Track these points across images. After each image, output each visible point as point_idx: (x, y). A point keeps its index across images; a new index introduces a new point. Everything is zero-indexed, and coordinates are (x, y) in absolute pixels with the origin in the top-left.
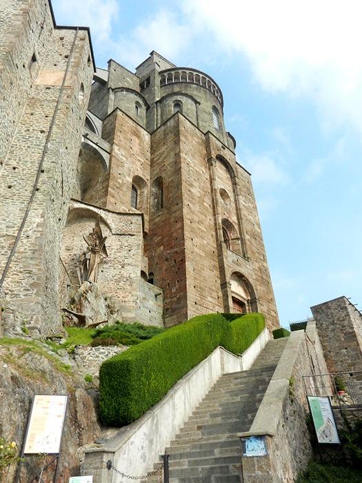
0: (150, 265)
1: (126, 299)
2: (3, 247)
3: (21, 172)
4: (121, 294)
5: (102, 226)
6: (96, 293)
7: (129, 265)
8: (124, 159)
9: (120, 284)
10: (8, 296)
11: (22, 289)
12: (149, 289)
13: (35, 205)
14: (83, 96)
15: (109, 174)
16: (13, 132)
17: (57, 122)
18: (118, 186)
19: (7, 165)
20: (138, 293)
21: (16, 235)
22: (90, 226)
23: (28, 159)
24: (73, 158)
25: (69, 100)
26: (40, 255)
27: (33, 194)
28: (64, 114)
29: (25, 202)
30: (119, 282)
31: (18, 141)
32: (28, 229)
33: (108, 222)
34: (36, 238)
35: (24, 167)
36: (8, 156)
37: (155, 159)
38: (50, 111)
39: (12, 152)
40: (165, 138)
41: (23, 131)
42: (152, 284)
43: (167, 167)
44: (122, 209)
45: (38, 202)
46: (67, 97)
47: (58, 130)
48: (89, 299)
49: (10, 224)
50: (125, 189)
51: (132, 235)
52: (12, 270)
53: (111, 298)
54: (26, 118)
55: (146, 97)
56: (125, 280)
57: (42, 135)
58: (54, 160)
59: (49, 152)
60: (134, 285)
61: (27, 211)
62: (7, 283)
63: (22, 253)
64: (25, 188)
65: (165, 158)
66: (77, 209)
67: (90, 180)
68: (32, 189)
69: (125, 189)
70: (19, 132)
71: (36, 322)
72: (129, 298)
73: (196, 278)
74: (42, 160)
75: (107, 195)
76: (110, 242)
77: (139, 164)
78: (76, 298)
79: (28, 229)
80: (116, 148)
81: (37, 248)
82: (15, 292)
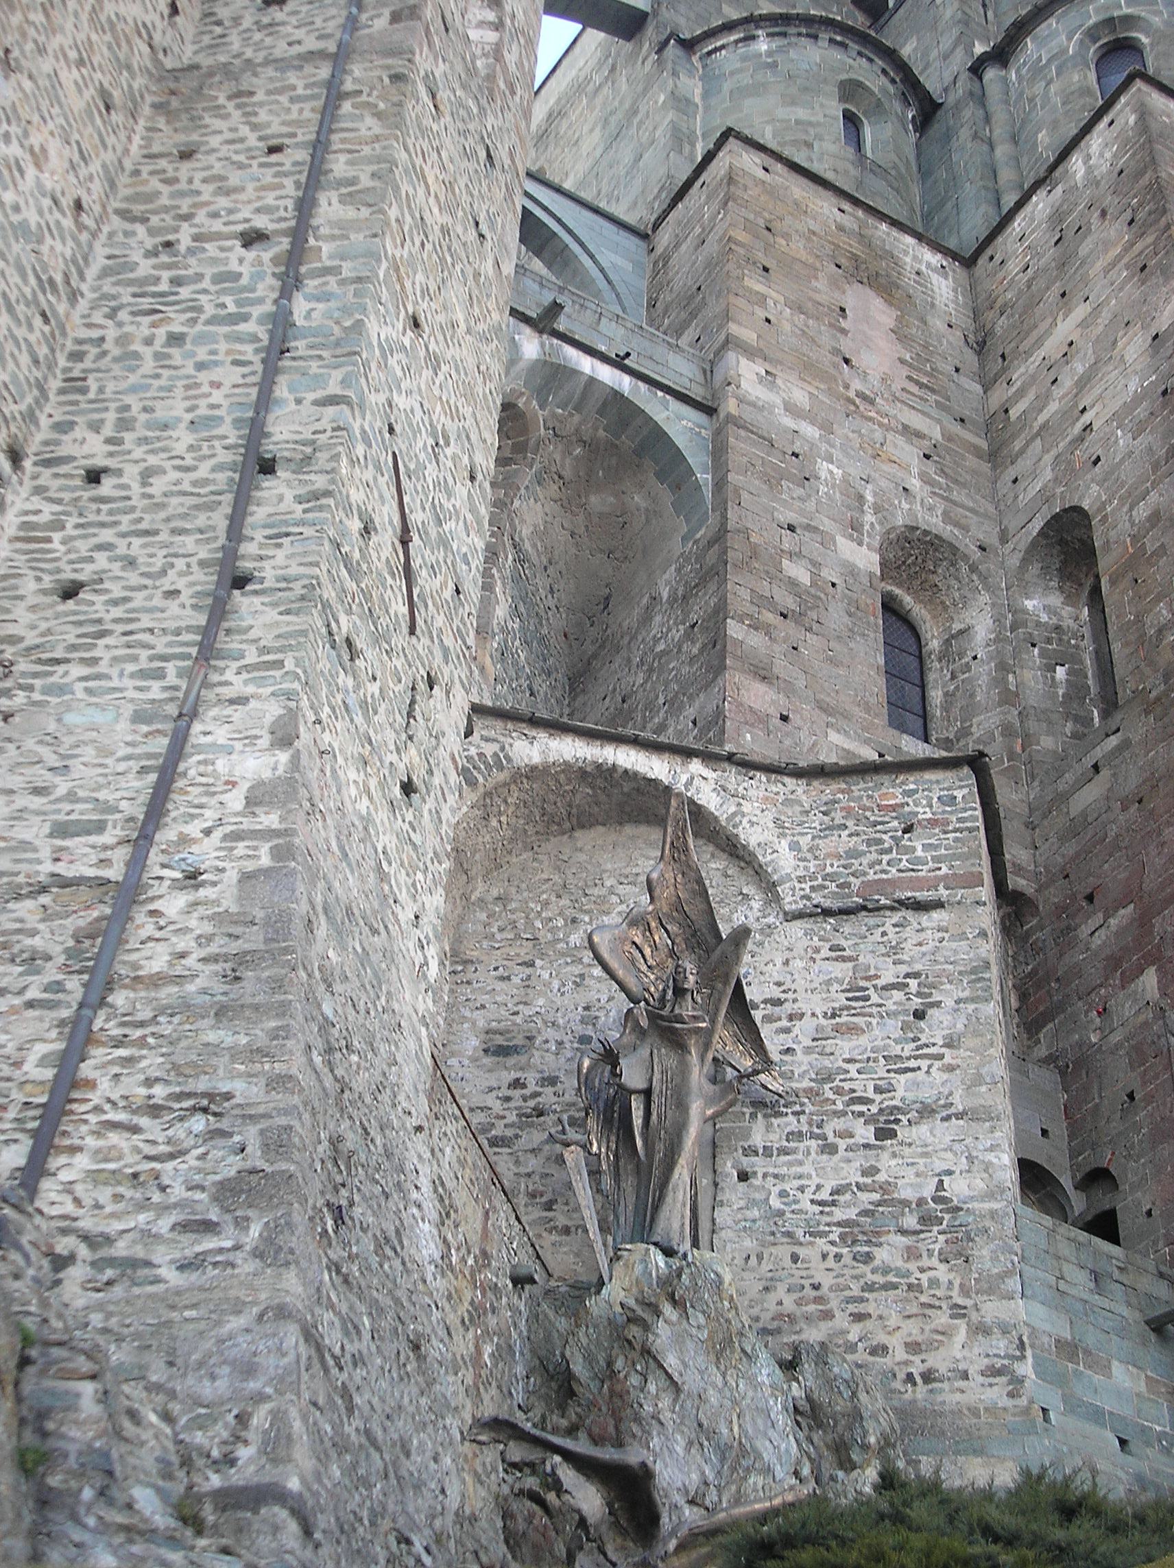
0: (1077, 1119)
1: (938, 1361)
2: (33, 961)
3: (136, 490)
4: (894, 1325)
5: (713, 867)
6: (715, 1317)
7: (926, 1111)
8: (810, 431)
10: (76, 1274)
11: (164, 1225)
12: (1097, 1277)
13: (233, 680)
14: (498, 26)
15: (720, 536)
16: (80, 262)
17: (339, 166)
18: (790, 603)
19: (47, 463)
20: (1019, 1310)
21: (115, 873)
22: (624, 873)
23: (176, 408)
24: (468, 394)
25: (399, 33)
26: (278, 985)
27: (219, 611)
28: (378, 115)
29: (171, 668)
30: (875, 1237)
31: (112, 315)
32: (194, 829)
33: (751, 836)
34: (246, 877)
35: (153, 460)
36: (52, 411)
37: (1014, 413)
38: (288, 111)
39: (75, 385)
40: (1062, 265)
41: (136, 256)
42: (1115, 1240)
43: (1109, 441)
44: (837, 744)
45: (252, 657)
46: (396, 18)
47: (350, 213)
48: (671, 1361)
49: (82, 812)
50: (836, 616)
51: (921, 907)
52: (96, 1098)
53: (822, 1353)
54: (155, 184)
55: (906, 51)
56: (911, 1221)
57: (250, 255)
58: (334, 389)
59: (300, 346)
60: (983, 1253)
62: (68, 1189)
63: (157, 980)
64: (166, 584)
65: (1083, 383)
66: (533, 773)
67: (607, 599)
68: (206, 579)
69: (836, 616)
70: (118, 267)
71: (276, 1447)
72: (959, 1350)
74: (265, 400)
75: (722, 668)
76: (775, 972)
77: (910, 454)
78: (578, 1367)
79: (193, 829)
80: (747, 374)
81: (253, 939)
82: (121, 1249)
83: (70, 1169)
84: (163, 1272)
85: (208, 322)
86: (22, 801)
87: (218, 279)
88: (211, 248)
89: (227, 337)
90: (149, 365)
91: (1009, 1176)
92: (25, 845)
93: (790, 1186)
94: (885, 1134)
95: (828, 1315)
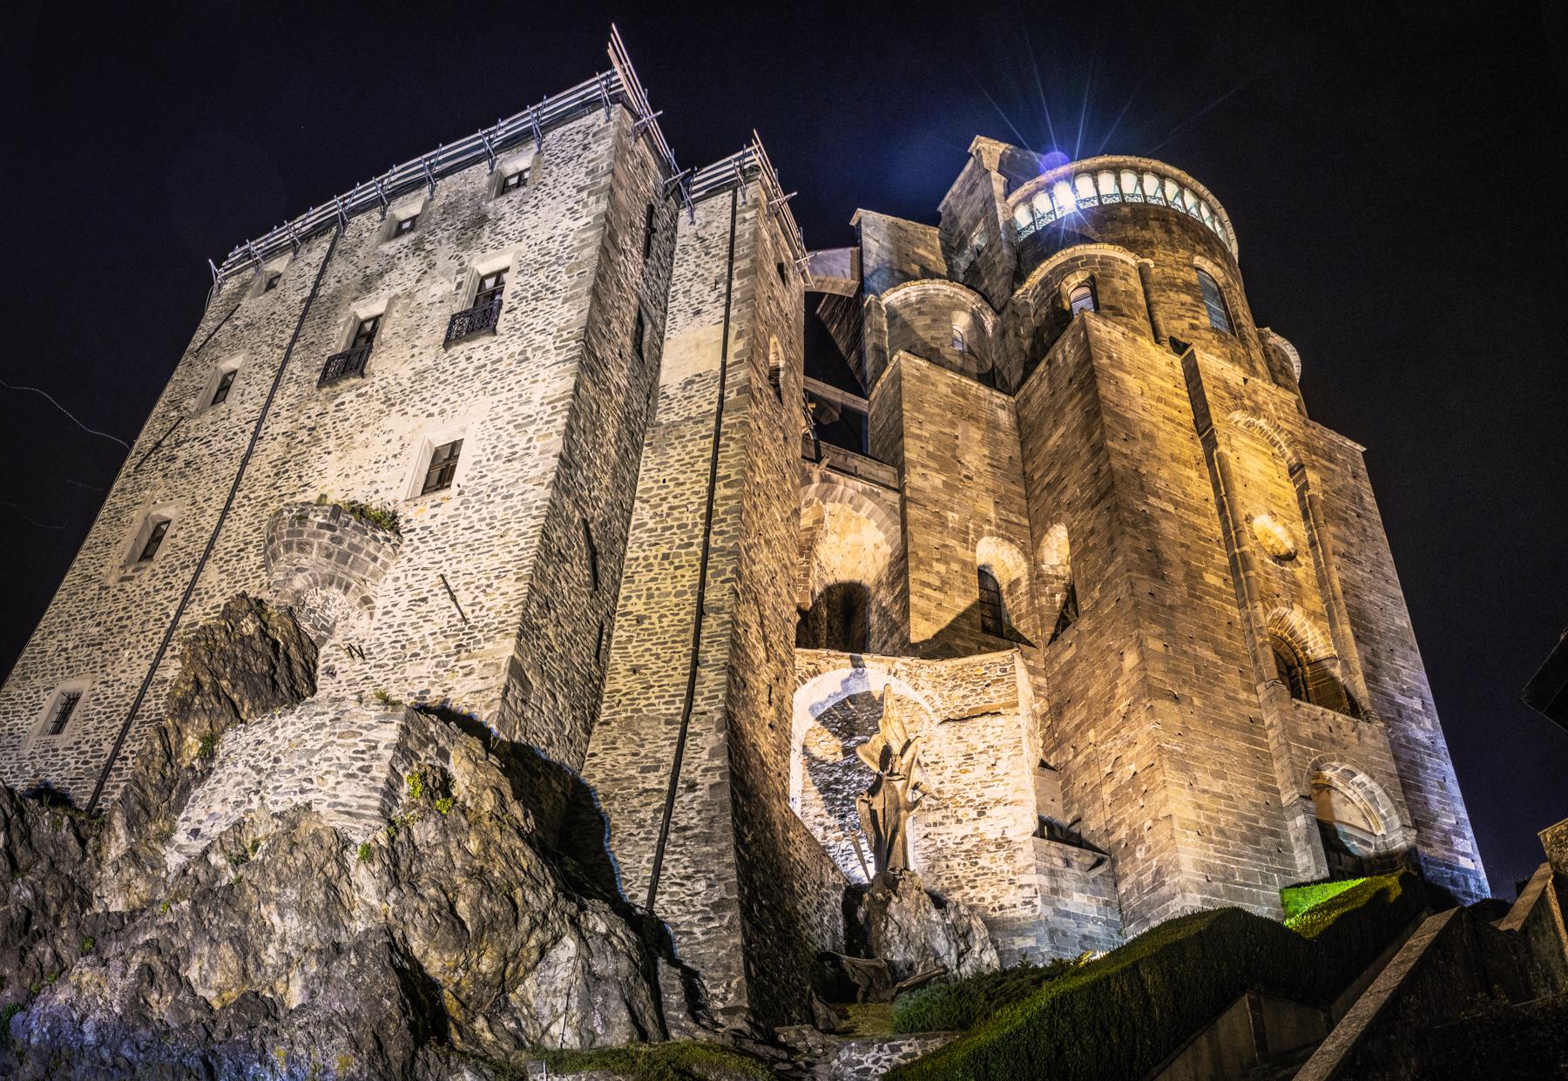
1: (1005, 901)
7: (998, 802)
9: (981, 863)
17: (721, 472)
35: (663, 611)
45: (707, 694)
48: (897, 917)
49: (649, 763)
56: (992, 848)
58: (728, 575)
61: (686, 721)
63: (685, 829)
68: (688, 661)
73: (1200, 807)
74: (703, 584)
76: (936, 750)
83: (661, 900)
84: (699, 935)
85: (680, 547)
86: (629, 758)
87: (679, 527)
88: (676, 513)
89: (687, 554)
90: (656, 569)
91: (1033, 826)
92: (631, 777)
93: (944, 837)
94: (981, 814)
95: (961, 888)
